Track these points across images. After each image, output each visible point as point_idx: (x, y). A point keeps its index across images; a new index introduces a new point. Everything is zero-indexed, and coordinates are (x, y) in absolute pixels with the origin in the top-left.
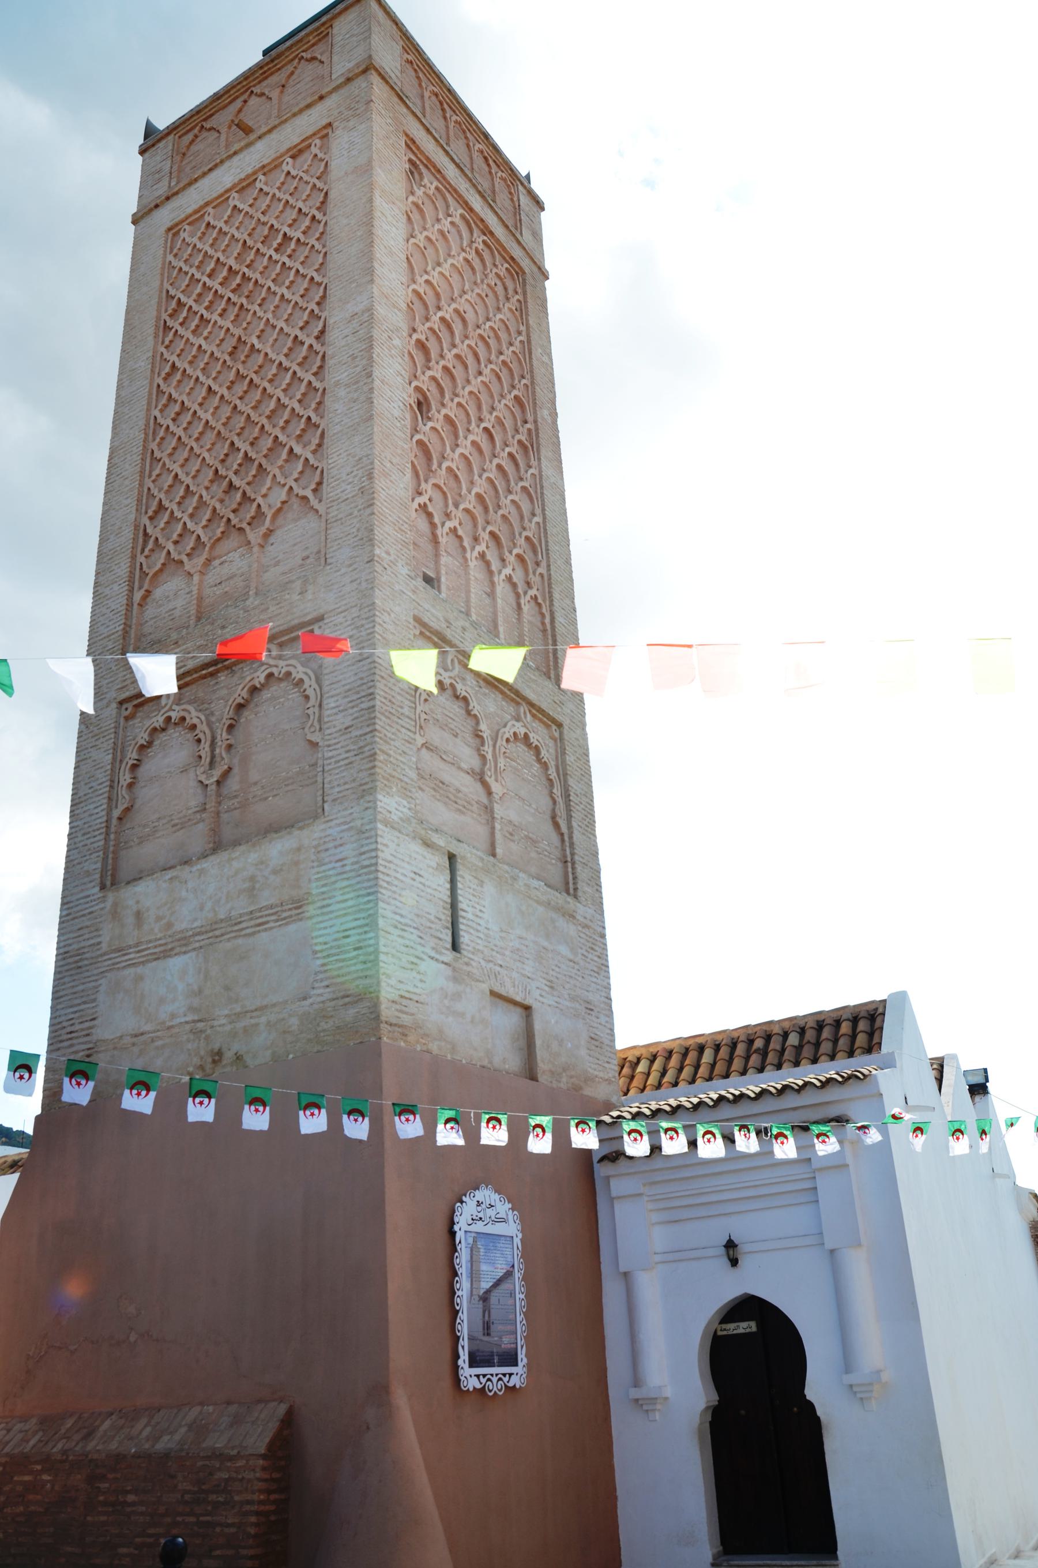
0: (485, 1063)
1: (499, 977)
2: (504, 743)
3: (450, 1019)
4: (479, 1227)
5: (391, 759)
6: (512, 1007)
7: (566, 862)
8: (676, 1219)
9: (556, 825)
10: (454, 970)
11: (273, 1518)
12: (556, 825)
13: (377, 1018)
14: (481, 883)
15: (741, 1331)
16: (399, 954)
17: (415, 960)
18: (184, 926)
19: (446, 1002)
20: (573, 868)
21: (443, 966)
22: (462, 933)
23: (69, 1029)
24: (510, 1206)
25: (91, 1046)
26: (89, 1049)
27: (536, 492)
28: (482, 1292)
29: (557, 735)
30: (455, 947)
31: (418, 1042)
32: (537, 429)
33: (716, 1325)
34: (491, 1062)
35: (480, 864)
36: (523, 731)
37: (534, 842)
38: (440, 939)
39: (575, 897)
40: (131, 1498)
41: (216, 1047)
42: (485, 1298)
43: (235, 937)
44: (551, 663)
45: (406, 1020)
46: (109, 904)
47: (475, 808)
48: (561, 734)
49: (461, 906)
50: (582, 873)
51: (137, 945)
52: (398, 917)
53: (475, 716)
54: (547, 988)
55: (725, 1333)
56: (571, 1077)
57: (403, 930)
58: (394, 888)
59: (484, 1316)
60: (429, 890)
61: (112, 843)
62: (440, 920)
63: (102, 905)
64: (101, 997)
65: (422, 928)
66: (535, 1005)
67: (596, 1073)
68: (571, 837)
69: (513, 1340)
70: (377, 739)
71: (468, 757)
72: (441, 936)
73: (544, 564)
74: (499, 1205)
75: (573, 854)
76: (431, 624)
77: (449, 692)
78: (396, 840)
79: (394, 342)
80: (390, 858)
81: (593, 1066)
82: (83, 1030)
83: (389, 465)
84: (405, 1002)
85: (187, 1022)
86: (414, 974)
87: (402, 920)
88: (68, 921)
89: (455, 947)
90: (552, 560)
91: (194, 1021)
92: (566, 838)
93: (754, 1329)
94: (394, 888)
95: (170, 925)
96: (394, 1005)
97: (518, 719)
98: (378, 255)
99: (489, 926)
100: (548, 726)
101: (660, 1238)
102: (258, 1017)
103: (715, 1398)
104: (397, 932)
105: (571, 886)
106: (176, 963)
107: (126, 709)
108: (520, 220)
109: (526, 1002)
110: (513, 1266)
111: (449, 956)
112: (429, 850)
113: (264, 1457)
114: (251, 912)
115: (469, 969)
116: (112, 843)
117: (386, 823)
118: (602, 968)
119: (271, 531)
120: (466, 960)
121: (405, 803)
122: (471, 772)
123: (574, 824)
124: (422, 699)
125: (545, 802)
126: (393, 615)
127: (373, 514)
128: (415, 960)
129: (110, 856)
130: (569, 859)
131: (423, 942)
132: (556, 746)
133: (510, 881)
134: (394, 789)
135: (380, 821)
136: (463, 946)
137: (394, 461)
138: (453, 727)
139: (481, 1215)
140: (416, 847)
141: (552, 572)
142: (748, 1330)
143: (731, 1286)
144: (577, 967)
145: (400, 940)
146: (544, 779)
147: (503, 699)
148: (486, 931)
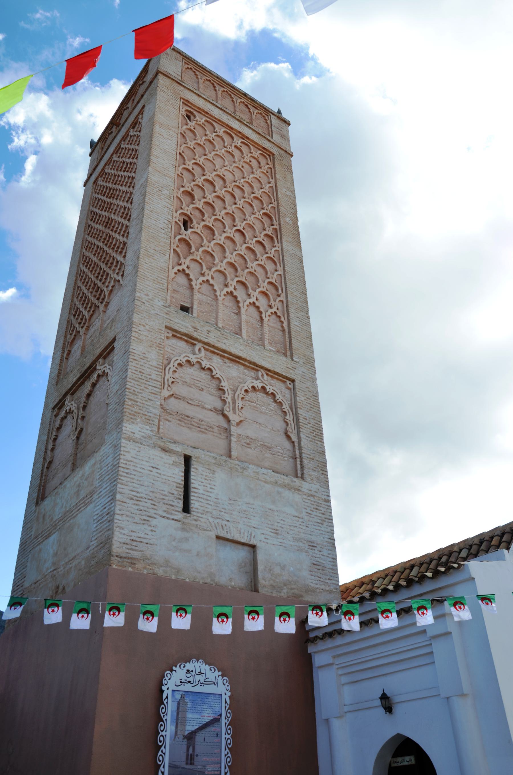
0: (208, 581)
1: (225, 528)
2: (243, 392)
3: (177, 554)
4: (188, 687)
5: (138, 404)
6: (240, 547)
7: (296, 458)
8: (356, 680)
9: (288, 437)
10: (184, 523)
12: (288, 437)
13: (110, 554)
14: (214, 472)
15: (406, 763)
16: (133, 515)
19: (174, 543)
20: (301, 461)
21: (174, 521)
24: (220, 673)
28: (186, 733)
29: (291, 386)
30: (186, 509)
31: (145, 568)
32: (280, 228)
33: (389, 759)
34: (214, 581)
35: (214, 461)
36: (260, 385)
37: (269, 448)
38: (172, 506)
39: (302, 478)
42: (190, 737)
44: (288, 347)
45: (135, 554)
47: (216, 429)
48: (294, 385)
49: (192, 485)
53: (218, 378)
54: (272, 534)
55: (396, 765)
56: (292, 589)
58: (133, 476)
59: (188, 750)
60: (164, 477)
61: (43, 481)
62: (173, 494)
64: (29, 564)
65: (155, 499)
66: (258, 545)
67: (317, 586)
68: (300, 444)
69: (217, 768)
70: (127, 393)
71: (211, 400)
72: (173, 504)
74: (208, 672)
75: (301, 453)
76: (180, 330)
77: (197, 366)
78: (137, 449)
79: (163, 192)
80: (131, 459)
81: (314, 582)
83: (152, 251)
84: (135, 543)
86: (146, 526)
87: (138, 495)
89: (186, 509)
90: (289, 293)
92: (296, 444)
93: (413, 762)
94: (133, 476)
95: (52, 519)
96: (125, 546)
97: (257, 379)
98: (155, 153)
99: (219, 497)
100: (284, 382)
101: (348, 694)
105: (299, 472)
108: (272, 131)
109: (251, 543)
110: (221, 715)
111: (180, 516)
112: (167, 454)
115: (197, 523)
116: (43, 481)
117: (129, 439)
119: (108, 303)
120: (195, 518)
121: (148, 427)
122: (216, 410)
123: (302, 435)
124: (171, 370)
125: (279, 425)
126: (147, 327)
127: (137, 276)
129: (42, 488)
130: (298, 456)
131: (155, 507)
132: (291, 392)
133: (240, 470)
134: (139, 420)
135: (125, 438)
136: (192, 509)
137: (157, 249)
138: (199, 385)
139: (191, 679)
140: (157, 453)
141: (289, 299)
142: (410, 763)
143: (387, 729)
144: (301, 520)
145: (134, 507)
146: (279, 412)
147: (245, 369)
148: (215, 500)
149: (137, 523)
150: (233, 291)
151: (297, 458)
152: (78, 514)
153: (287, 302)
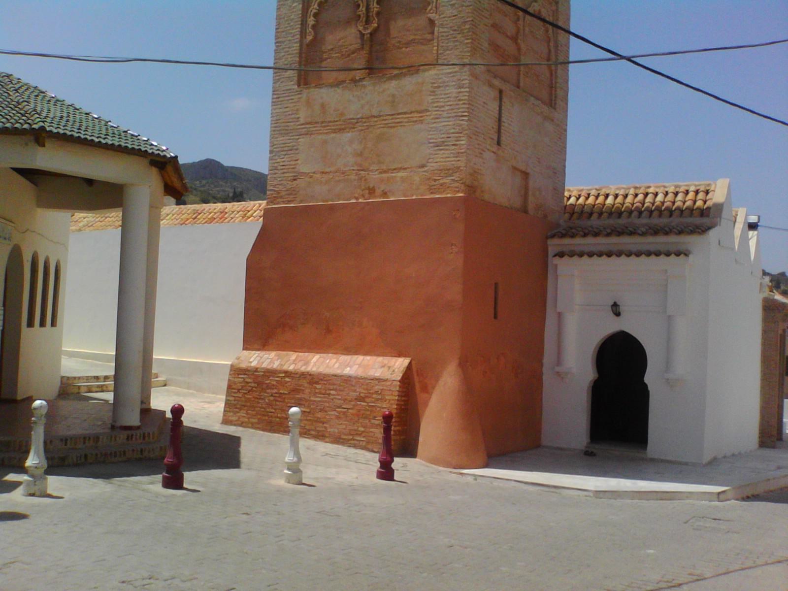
7: (552, 87)
11: (403, 407)
17: (482, 152)
23: (282, 164)
25: (296, 175)
26: (295, 176)
30: (499, 143)
39: (555, 109)
40: (333, 392)
41: (371, 186)
46: (304, 96)
50: (560, 93)
51: (322, 122)
63: (300, 96)
68: (556, 73)
85: (353, 170)
89: (499, 143)
91: (358, 170)
92: (554, 73)
103: (596, 376)
105: (553, 102)
106: (347, 136)
113: (400, 381)
118: (563, 150)
128: (482, 152)
140: (485, 88)
151: (552, 87)
152: (397, 126)
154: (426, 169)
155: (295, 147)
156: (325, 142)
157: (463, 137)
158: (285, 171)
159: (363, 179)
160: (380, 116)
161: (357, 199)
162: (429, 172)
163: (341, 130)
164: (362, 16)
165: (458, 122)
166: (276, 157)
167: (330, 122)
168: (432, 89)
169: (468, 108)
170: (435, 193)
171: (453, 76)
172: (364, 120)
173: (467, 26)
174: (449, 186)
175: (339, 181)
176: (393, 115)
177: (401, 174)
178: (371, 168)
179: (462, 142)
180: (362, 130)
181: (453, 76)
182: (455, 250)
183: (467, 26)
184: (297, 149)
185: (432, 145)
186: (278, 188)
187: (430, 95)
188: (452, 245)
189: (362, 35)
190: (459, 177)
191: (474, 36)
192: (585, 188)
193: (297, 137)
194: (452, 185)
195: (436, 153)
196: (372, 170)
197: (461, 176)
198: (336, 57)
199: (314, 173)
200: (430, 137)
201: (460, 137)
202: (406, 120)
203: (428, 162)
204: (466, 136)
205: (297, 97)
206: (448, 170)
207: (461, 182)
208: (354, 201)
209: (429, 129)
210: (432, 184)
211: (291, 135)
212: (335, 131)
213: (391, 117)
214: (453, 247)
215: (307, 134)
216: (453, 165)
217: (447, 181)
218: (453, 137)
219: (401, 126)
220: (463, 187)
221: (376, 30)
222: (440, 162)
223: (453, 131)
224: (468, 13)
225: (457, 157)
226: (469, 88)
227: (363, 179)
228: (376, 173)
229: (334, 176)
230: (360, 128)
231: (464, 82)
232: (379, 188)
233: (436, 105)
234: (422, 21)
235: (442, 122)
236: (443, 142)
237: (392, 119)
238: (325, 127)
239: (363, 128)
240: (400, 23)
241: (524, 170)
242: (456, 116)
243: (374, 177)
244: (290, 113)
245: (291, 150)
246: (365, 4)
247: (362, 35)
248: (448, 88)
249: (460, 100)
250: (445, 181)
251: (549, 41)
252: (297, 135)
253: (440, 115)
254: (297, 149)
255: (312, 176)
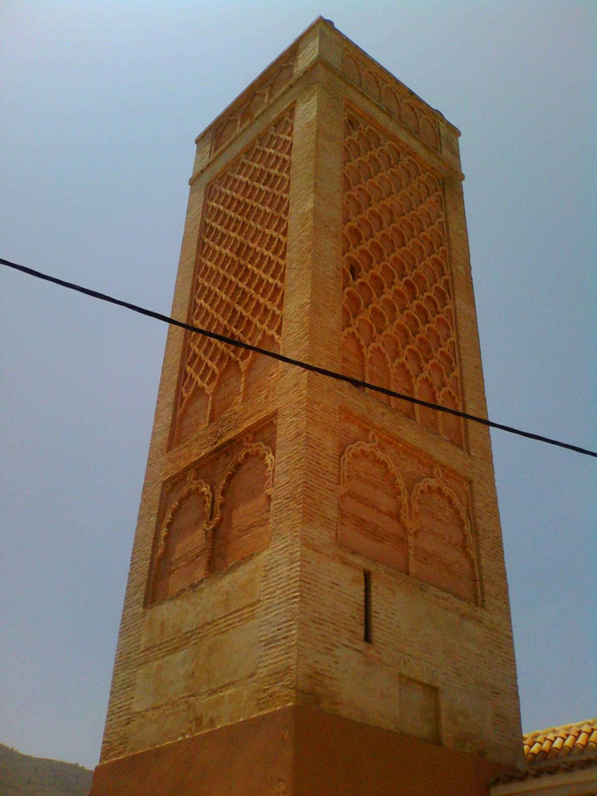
0: (392, 727)
5: (316, 502)
10: (366, 656)
12: (467, 555)
18: (187, 629)
22: (374, 629)
27: (452, 322)
30: (368, 638)
32: (452, 279)
38: (353, 632)
39: (484, 607)
43: (215, 635)
45: (320, 690)
48: (471, 488)
49: (373, 608)
51: (160, 645)
52: (316, 615)
57: (320, 624)
62: (354, 618)
63: (143, 619)
68: (479, 563)
72: (356, 630)
73: (457, 369)
75: (481, 575)
82: (126, 705)
85: (183, 697)
87: (321, 617)
88: (125, 631)
89: (368, 638)
92: (476, 563)
94: (314, 593)
95: (179, 630)
102: (224, 691)
104: (315, 625)
105: (479, 599)
106: (181, 655)
107: (167, 487)
111: (361, 645)
114: (225, 617)
118: (510, 661)
121: (326, 532)
122: (390, 514)
123: (482, 553)
126: (322, 406)
128: (331, 647)
131: (338, 633)
134: (317, 523)
136: (374, 639)
141: (464, 375)
149: (320, 652)
150: (406, 362)
151: (475, 580)
152: (229, 630)
153: (462, 378)
154: (255, 677)
155: (133, 682)
156: (160, 668)
157: (294, 624)
158: (121, 714)
159: (192, 707)
160: (214, 621)
161: (184, 735)
162: (259, 681)
163: (176, 649)
164: (207, 512)
165: (289, 606)
166: (115, 699)
167: (167, 642)
168: (264, 574)
169: (299, 586)
170: (263, 709)
171: (286, 551)
172: (198, 631)
173: (299, 490)
174: (278, 695)
175: (169, 715)
176: (225, 617)
177: (231, 691)
178: (202, 690)
179: (294, 632)
180: (195, 644)
181: (286, 551)
182: (283, 787)
183: (299, 490)
184: (134, 684)
185: (263, 644)
186: (112, 737)
187: (263, 581)
188: (280, 781)
189: (207, 532)
190: (289, 680)
191: (309, 500)
192: (574, 724)
193: (135, 669)
194: (281, 694)
195: (266, 653)
196: (202, 692)
197: (292, 678)
198: (183, 565)
199: (147, 710)
200: (260, 634)
201: (291, 625)
202: (238, 619)
203: (257, 668)
204: (297, 622)
205: (141, 621)
206: (278, 673)
207: (291, 686)
208: (180, 738)
209: (261, 624)
210: (261, 697)
211: (131, 667)
212: (170, 653)
213: (223, 620)
214: (280, 784)
215: (144, 663)
216: (283, 665)
217: (277, 689)
218: (285, 627)
219: (233, 628)
220: (293, 693)
221: (218, 525)
222: (271, 664)
223: (284, 619)
224: (300, 475)
225: (287, 654)
226: (300, 560)
227: (192, 707)
228: (204, 696)
229: (164, 710)
230: (194, 642)
231: (296, 555)
232: (206, 716)
233: (267, 592)
234: (262, 500)
235: (272, 611)
236: (274, 637)
237: (225, 621)
238: (162, 649)
239: (196, 641)
240: (242, 508)
241: (426, 681)
242: (287, 600)
243: (203, 701)
244: (133, 641)
245: (128, 687)
246: (211, 500)
247: (207, 532)
248: (280, 567)
249: (291, 579)
250: (276, 688)
251: (462, 525)
252: (136, 667)
253: (271, 603)
254: (134, 684)
255: (144, 715)
